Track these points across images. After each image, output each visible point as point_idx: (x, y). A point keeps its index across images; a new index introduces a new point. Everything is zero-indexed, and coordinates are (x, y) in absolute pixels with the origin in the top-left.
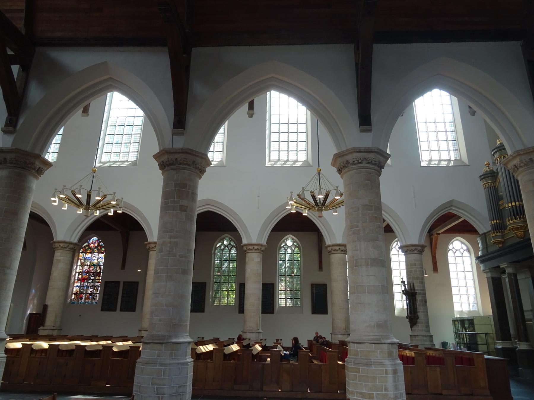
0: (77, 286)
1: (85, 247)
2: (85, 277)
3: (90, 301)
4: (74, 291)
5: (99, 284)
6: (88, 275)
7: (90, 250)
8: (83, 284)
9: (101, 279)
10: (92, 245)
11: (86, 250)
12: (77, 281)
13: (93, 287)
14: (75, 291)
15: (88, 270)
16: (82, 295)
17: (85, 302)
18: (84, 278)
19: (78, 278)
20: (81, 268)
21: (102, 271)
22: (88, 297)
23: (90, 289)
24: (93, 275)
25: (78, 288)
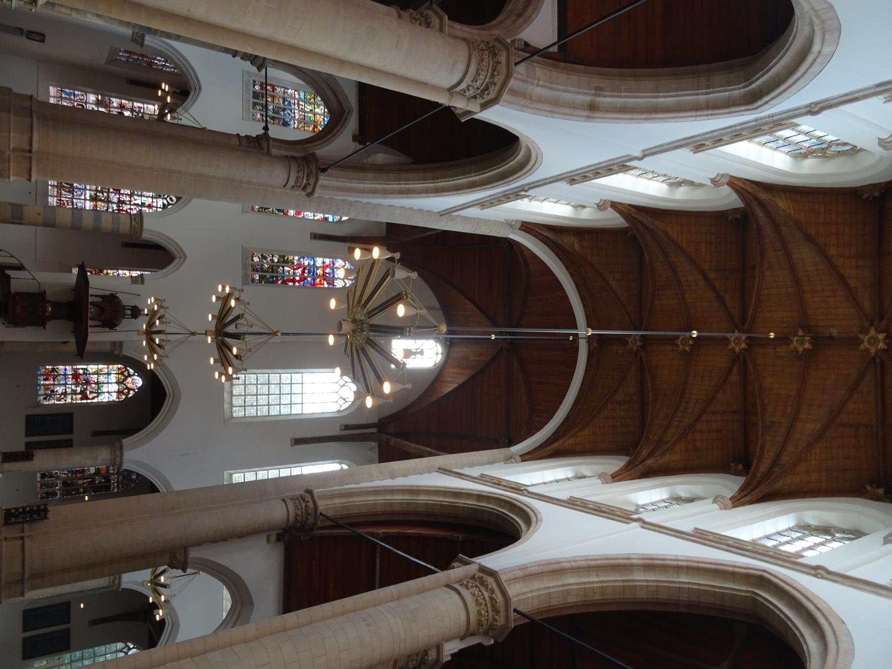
0: (66, 370)
1: (128, 370)
2: (80, 379)
3: (42, 392)
4: (58, 367)
5: (69, 400)
6: (84, 382)
7: (122, 378)
8: (69, 378)
9: (77, 402)
10: (129, 380)
11: (122, 373)
12: (74, 369)
13: (65, 394)
14: (58, 368)
15: (91, 382)
16: (52, 380)
17: (40, 385)
18: (79, 378)
19: (79, 369)
20: (94, 370)
21: (89, 401)
22: (48, 388)
23: (61, 390)
24: (83, 389)
25: (64, 371)
